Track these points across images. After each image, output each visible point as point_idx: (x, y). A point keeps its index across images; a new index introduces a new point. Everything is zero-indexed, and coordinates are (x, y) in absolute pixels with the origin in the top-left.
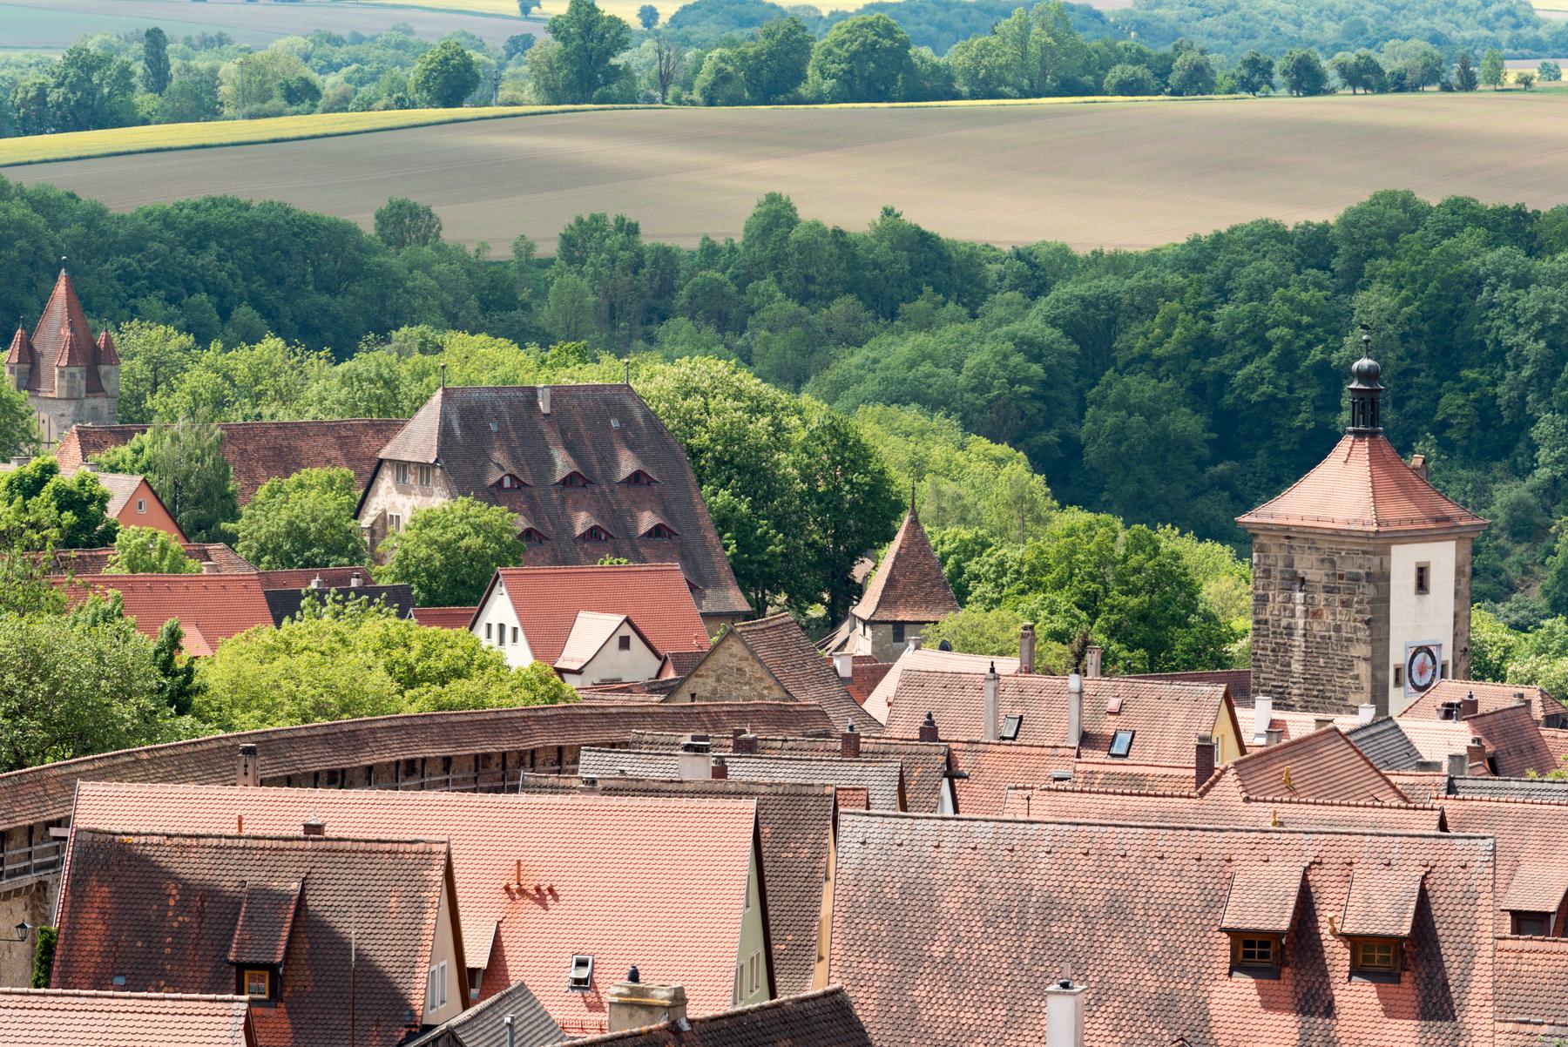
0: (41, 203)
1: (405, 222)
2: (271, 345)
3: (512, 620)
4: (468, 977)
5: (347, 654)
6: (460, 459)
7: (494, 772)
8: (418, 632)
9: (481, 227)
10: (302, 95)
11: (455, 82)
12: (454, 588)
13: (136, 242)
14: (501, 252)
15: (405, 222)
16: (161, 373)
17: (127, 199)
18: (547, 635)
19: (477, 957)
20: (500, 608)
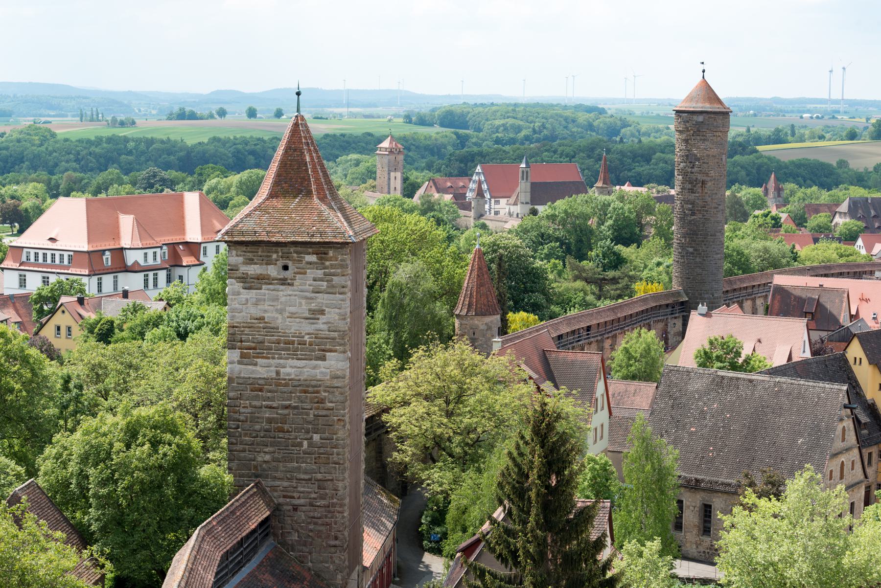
0: (769, 159)
1: (842, 164)
2: (815, 188)
3: (862, 245)
4: (851, 316)
5: (828, 251)
6: (852, 211)
7: (858, 275)
8: (843, 247)
9: (858, 165)
10: (822, 138)
11: (853, 136)
12: (850, 238)
13: (786, 167)
14: (862, 170)
15: (842, 164)
16: (792, 193)
17: (785, 159)
18: (869, 248)
19: (853, 312)
20: (860, 242)
